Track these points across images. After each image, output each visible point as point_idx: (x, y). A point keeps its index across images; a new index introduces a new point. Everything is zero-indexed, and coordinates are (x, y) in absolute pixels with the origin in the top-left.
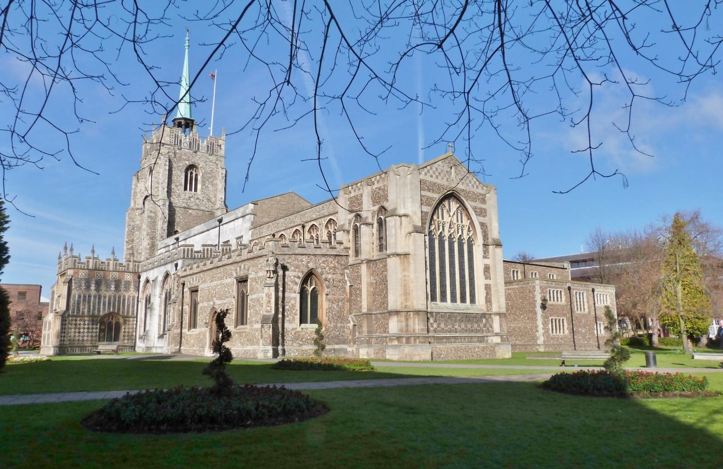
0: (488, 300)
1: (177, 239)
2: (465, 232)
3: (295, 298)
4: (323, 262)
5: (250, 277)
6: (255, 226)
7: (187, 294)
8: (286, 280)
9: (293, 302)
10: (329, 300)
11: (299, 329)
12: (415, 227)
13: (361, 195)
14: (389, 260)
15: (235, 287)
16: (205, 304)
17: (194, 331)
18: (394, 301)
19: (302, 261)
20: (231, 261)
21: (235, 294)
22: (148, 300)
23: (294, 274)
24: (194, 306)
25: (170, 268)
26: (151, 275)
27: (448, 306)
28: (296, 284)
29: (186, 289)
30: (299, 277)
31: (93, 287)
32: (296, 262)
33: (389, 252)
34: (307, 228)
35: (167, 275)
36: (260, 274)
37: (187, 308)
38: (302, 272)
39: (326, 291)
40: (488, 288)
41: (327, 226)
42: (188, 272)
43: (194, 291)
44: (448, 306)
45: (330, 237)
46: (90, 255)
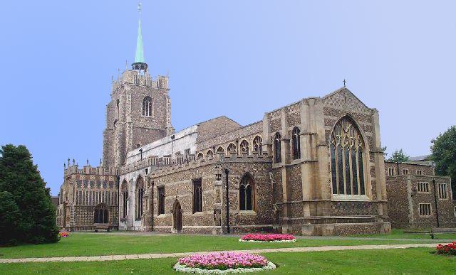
0: (374, 192)
1: (141, 150)
2: (356, 145)
5: (204, 178)
6: (199, 142)
7: (156, 191)
8: (229, 181)
12: (321, 142)
13: (280, 120)
14: (302, 166)
15: (192, 185)
16: (170, 197)
18: (306, 194)
20: (189, 167)
21: (192, 190)
22: (126, 195)
25: (141, 172)
26: (128, 177)
27: (344, 197)
29: (155, 187)
31: (89, 187)
33: (302, 160)
34: (240, 143)
35: (140, 178)
36: (211, 177)
37: (156, 200)
38: (241, 174)
39: (257, 187)
40: (374, 183)
41: (254, 142)
42: (156, 176)
43: (161, 189)
44: (344, 197)
45: (256, 149)
46: (86, 164)
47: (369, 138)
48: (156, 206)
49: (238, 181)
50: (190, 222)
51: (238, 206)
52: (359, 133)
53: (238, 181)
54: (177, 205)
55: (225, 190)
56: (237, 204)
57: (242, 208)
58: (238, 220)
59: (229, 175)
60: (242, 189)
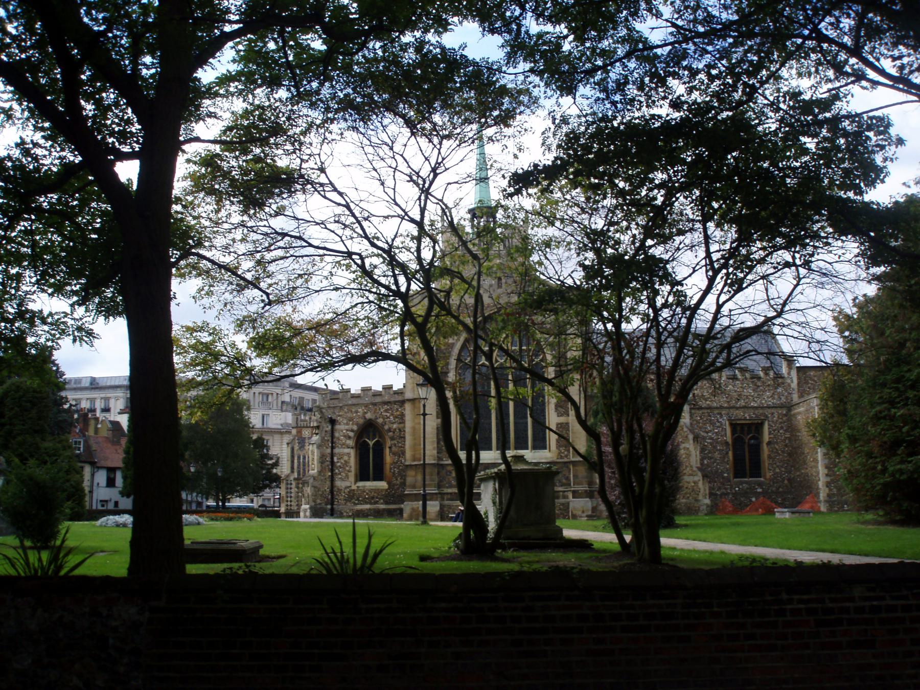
3: (349, 454)
4: (386, 411)
8: (337, 435)
10: (394, 454)
11: (354, 487)
19: (357, 412)
23: (347, 427)
28: (350, 438)
30: (352, 431)
32: (349, 415)
38: (357, 424)
39: (389, 443)
49: (351, 434)
53: (351, 434)
56: (349, 471)
57: (363, 476)
58: (352, 496)
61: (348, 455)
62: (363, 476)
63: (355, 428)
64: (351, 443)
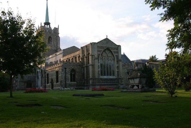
9: (68, 77)
17: (48, 84)
24: (48, 78)
37: (46, 79)
39: (77, 74)
47: (116, 56)
48: (46, 81)
50: (56, 86)
51: (70, 80)
52: (113, 54)
54: (52, 80)
55: (65, 75)
57: (71, 81)
59: (66, 70)
60: (71, 75)
61: (69, 76)
62: (71, 81)
63: (70, 70)
64: (69, 73)
